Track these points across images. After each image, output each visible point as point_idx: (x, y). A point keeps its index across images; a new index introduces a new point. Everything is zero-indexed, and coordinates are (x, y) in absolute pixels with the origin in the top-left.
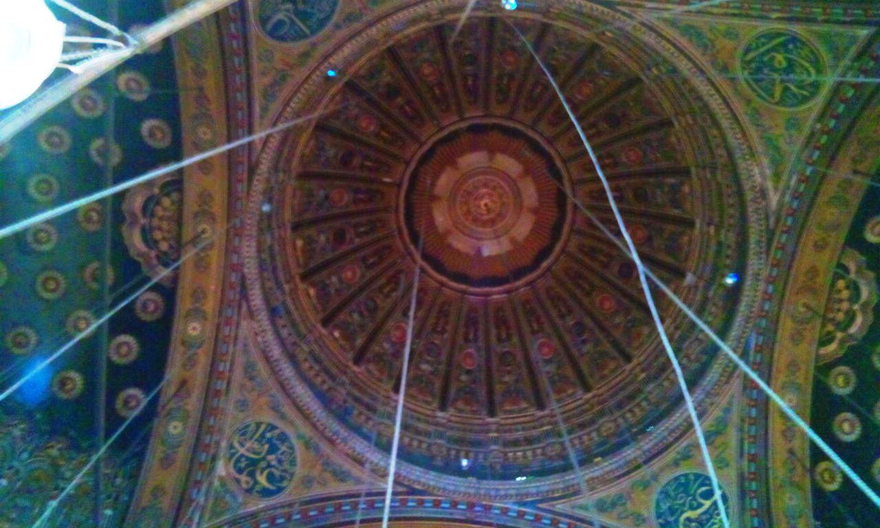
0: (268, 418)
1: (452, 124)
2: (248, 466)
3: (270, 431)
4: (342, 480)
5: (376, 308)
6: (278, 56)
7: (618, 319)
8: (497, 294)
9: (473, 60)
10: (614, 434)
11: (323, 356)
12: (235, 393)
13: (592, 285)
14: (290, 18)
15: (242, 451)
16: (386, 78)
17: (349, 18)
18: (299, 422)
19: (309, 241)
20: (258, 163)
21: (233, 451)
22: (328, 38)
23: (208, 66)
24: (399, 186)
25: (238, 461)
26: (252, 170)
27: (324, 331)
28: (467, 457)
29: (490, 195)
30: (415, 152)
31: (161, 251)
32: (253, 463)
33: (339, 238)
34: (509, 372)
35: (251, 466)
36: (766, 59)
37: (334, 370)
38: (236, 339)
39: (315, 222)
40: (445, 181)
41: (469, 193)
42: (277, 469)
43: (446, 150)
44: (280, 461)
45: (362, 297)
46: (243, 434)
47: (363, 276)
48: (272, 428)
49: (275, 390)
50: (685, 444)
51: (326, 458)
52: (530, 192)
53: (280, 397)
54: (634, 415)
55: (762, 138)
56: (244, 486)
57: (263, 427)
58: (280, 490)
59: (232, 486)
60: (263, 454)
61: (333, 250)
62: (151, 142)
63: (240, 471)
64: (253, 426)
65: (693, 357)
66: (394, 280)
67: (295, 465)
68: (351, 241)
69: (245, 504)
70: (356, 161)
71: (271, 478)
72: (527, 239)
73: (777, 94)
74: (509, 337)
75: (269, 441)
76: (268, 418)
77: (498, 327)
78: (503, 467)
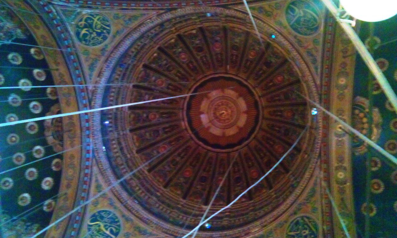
0: (113, 29)
1: (257, 92)
5: (170, 71)
7: (182, 180)
8: (184, 124)
9: (287, 98)
10: (131, 187)
11: (145, 50)
12: (121, 13)
13: (194, 166)
14: (296, 15)
15: (96, 20)
16: (273, 60)
17: (299, 42)
18: (113, 44)
19: (195, 36)
20: (230, 9)
21: (95, 16)
22: (290, 33)
24: (227, 73)
25: (91, 19)
27: (156, 48)
28: (110, 123)
29: (228, 114)
30: (242, 77)
33: (200, 49)
34: (150, 135)
35: (89, 26)
36: (306, 226)
37: (138, 56)
38: (146, 9)
39: (205, 36)
40: (230, 93)
41: (227, 105)
43: (245, 92)
44: (93, 38)
45: (174, 64)
47: (183, 63)
48: (108, 33)
49: (126, 31)
50: (132, 218)
51: (98, 59)
52: (231, 132)
54: (141, 193)
55: (272, 229)
57: (108, 28)
58: (80, 40)
59: (79, 17)
61: (194, 47)
63: (86, 21)
64: (108, 23)
65: (171, 215)
66: (183, 78)
68: (198, 55)
69: (71, 25)
70: (235, 52)
71: (85, 35)
72: (210, 133)
73: (292, 233)
74: (166, 133)
75: (102, 32)
76: (113, 29)
77: (170, 127)
78: (108, 140)
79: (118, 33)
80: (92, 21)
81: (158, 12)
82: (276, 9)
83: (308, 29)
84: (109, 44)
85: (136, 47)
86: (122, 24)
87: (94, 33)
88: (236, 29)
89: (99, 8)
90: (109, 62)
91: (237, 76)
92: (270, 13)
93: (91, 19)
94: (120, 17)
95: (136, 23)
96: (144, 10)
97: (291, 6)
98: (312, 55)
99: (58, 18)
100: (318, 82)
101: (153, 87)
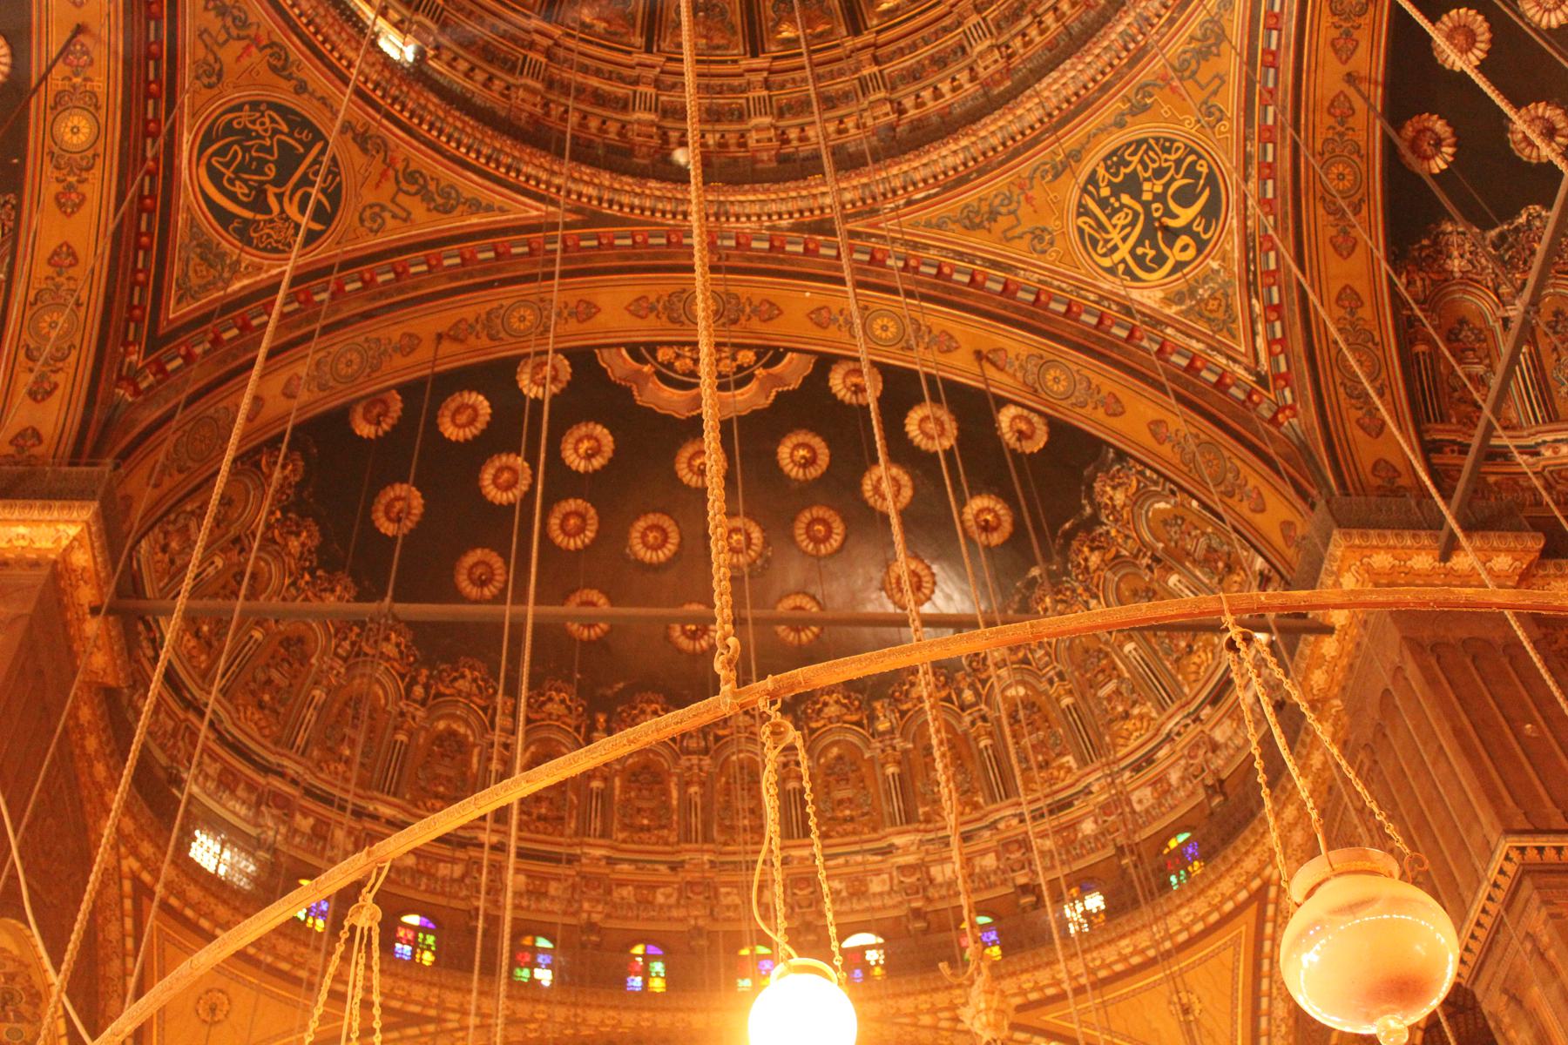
2: (1154, 246)
3: (1097, 188)
6: (369, 197)
12: (1016, 251)
15: (1124, 251)
21: (1121, 267)
23: (396, 333)
25: (1140, 261)
26: (593, 219)
31: (757, 362)
32: (1148, 234)
35: (1158, 232)
38: (915, 246)
42: (1172, 180)
44: (1159, 173)
46: (1094, 243)
48: (1092, 179)
56: (1191, 253)
58: (1211, 180)
59: (1180, 285)
60: (1139, 208)
63: (1160, 260)
67: (1172, 141)
75: (1116, 190)
79: (1054, 167)
80: (1140, 251)
81: (875, 226)
82: (383, 208)
83: (246, 133)
86: (1029, 199)
87: (1147, 197)
89: (1092, 297)
90: (1132, 46)
92: (405, 186)
94: (1029, 237)
95: (969, 197)
96: (926, 247)
99: (1257, 307)
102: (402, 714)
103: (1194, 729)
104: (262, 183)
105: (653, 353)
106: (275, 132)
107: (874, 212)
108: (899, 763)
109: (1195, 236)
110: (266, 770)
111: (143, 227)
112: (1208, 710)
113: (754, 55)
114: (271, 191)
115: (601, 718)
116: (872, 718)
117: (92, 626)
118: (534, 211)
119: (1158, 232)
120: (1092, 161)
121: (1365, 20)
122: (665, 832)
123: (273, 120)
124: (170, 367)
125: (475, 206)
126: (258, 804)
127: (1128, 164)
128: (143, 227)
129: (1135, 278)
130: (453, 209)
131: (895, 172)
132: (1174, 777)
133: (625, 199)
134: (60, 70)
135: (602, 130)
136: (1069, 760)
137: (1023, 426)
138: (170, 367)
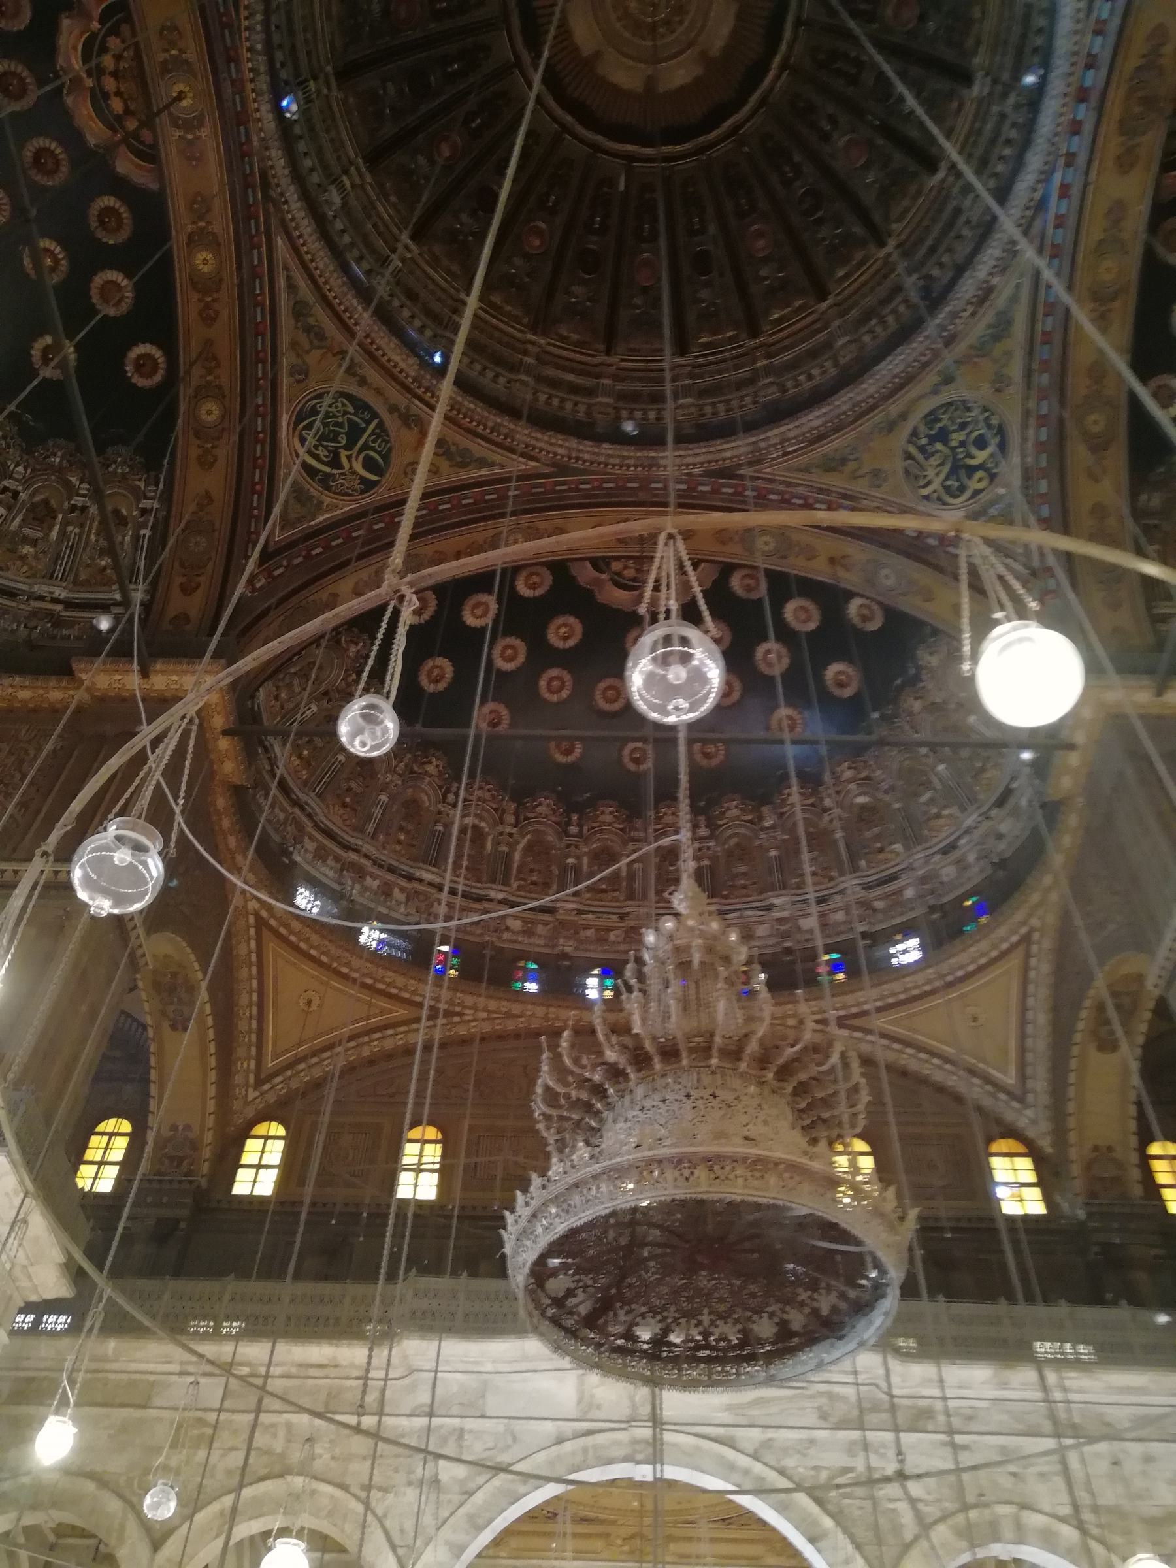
4: (1009, 322)
15: (936, 485)
22: (379, 391)
24: (630, 158)
25: (947, 489)
32: (953, 472)
35: (960, 469)
38: (789, 484)
40: (624, 75)
44: (963, 426)
48: (915, 433)
49: (866, 425)
53: (877, 417)
57: (913, 450)
58: (1001, 431)
59: (975, 506)
62: (539, 592)
63: (962, 489)
71: (981, 443)
80: (949, 483)
84: (922, 400)
85: (879, 329)
87: (954, 444)
88: (575, 337)
91: (596, 148)
93: (947, 489)
96: (799, 485)
97: (374, 478)
98: (308, 329)
100: (280, 242)
101: (880, 142)
102: (440, 813)
103: (986, 825)
104: (337, 448)
105: (608, 565)
106: (346, 413)
107: (759, 461)
108: (777, 848)
109: (987, 470)
110: (347, 847)
111: (257, 478)
112: (994, 813)
113: (682, 355)
114: (343, 454)
115: (575, 817)
116: (761, 818)
117: (224, 744)
118: (521, 465)
119: (960, 469)
120: (915, 419)
121: (1117, 304)
122: (616, 894)
123: (344, 405)
124: (276, 573)
125: (483, 463)
126: (342, 870)
127: (940, 420)
128: (257, 478)
129: (944, 504)
130: (469, 464)
131: (773, 434)
132: (971, 858)
133: (587, 457)
134: (197, 371)
135: (575, 411)
136: (898, 847)
137: (866, 612)
138: (276, 573)
